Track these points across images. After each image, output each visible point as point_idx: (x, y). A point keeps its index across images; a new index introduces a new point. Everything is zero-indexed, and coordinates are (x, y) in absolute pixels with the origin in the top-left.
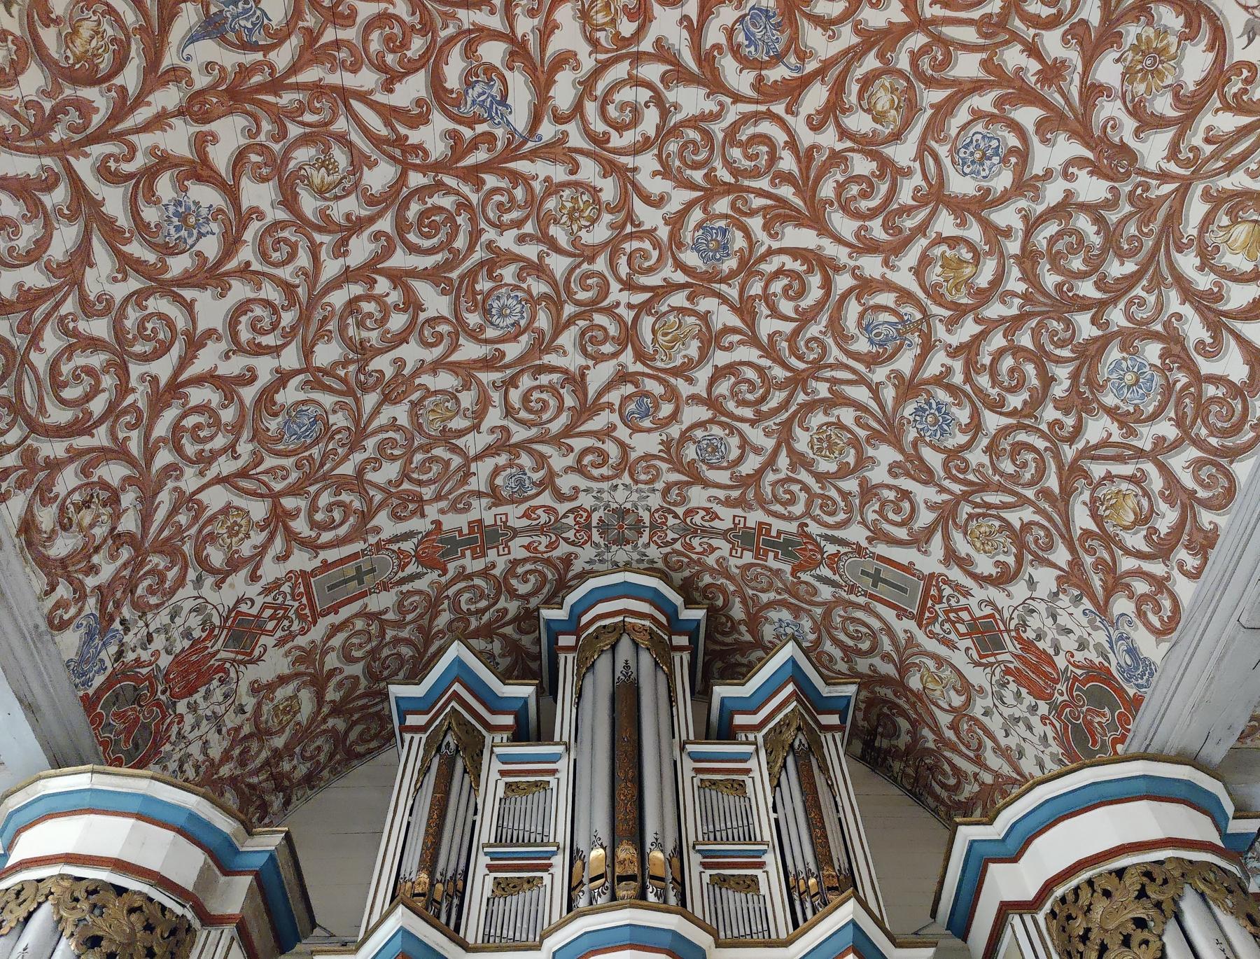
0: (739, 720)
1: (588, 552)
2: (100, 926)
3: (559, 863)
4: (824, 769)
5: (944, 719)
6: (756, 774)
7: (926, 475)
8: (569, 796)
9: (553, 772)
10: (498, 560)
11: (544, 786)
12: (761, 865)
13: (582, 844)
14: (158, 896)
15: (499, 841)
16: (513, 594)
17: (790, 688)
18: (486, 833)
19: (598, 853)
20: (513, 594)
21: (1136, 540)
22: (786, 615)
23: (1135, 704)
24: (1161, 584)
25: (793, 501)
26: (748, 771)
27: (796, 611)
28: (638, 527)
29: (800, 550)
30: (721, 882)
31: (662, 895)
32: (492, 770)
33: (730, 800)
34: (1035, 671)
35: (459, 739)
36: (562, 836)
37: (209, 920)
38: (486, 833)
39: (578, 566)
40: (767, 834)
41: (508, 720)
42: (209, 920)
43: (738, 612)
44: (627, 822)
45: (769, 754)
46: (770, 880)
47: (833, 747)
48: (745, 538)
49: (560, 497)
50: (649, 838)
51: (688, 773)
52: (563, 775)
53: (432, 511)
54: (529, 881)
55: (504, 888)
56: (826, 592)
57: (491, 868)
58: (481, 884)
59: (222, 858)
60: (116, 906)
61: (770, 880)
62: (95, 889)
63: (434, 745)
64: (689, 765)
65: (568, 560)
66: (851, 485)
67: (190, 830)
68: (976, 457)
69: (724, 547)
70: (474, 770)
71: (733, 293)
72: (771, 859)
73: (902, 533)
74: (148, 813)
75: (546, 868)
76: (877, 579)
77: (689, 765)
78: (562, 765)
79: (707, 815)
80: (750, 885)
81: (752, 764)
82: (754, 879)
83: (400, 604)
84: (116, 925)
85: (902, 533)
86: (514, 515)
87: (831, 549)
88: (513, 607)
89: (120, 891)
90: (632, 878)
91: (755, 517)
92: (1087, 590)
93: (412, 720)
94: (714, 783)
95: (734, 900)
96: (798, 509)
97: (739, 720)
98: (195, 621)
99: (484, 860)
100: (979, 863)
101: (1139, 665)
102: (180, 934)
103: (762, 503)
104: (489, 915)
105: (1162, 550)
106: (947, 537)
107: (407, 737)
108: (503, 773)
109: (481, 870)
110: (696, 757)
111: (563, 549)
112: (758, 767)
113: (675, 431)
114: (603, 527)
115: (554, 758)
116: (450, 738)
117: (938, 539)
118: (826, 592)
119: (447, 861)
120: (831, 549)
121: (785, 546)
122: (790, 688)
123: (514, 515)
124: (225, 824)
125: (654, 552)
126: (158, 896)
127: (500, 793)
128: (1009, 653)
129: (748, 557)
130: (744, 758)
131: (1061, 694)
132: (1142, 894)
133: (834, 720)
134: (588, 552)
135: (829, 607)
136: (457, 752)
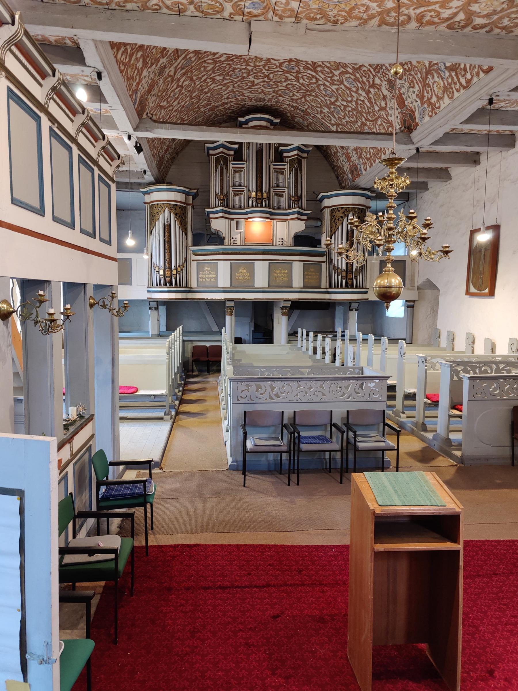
0: (285, 154)
1: (251, 103)
2: (177, 212)
3: (246, 190)
4: (301, 170)
5: (333, 151)
6: (286, 169)
7: (335, 117)
8: (248, 177)
9: (243, 168)
10: (227, 106)
11: (241, 171)
12: (284, 192)
13: (251, 189)
14: (182, 205)
15: (233, 186)
16: (230, 109)
17: (296, 152)
18: (231, 183)
19: (254, 194)
20: (230, 109)
21: (365, 154)
22: (301, 119)
23: (359, 175)
24: (366, 163)
25: (305, 105)
26: (284, 169)
27: (303, 120)
28: (265, 100)
29: (305, 112)
30: (276, 195)
31: (266, 202)
32: (230, 166)
33: (280, 176)
34: (349, 158)
35: (224, 162)
36: (246, 184)
37: (188, 204)
38: (231, 183)
39: (247, 105)
40: (287, 185)
41: (232, 153)
42: (188, 204)
43: (289, 115)
44: (259, 188)
45: (290, 165)
46: (286, 195)
47: (304, 163)
48: (293, 107)
49: (245, 96)
50: (264, 190)
51: (272, 169)
52: (246, 169)
53: (212, 104)
54: (240, 194)
55: (236, 195)
56: (311, 121)
57: (233, 191)
58: (231, 194)
59: (187, 194)
60: (177, 208)
61: (286, 195)
62: (174, 205)
63: (217, 161)
64: (272, 167)
65: (245, 104)
66: (319, 109)
67: (182, 192)
68: (344, 121)
69: (287, 107)
70: (227, 168)
71: (295, 75)
72: (286, 190)
73: (329, 121)
74: (176, 191)
75: (243, 191)
76: (322, 124)
77: (272, 167)
78: (245, 166)
79: (275, 179)
80: (282, 196)
81: (286, 167)
82: (283, 194)
83: (203, 118)
84: (178, 211)
85: (329, 121)
86: (232, 100)
87: (312, 115)
88: (230, 111)
89: (177, 205)
90: (260, 199)
91: (294, 105)
92: (357, 154)
93: (211, 152)
94: (277, 172)
95: (278, 198)
96: (306, 107)
97: (285, 154)
98: (168, 144)
99: (231, 189)
100: (323, 198)
101: (361, 170)
102: (185, 208)
103: (297, 103)
104: (233, 200)
105: (368, 159)
106: (337, 127)
107: (210, 156)
108: (233, 167)
109: (231, 191)
110: (274, 165)
111: (244, 103)
112: (287, 167)
113: (277, 89)
114: (255, 100)
115: (243, 164)
116: (222, 163)
117: (335, 127)
118: (311, 121)
119: (225, 192)
120: (312, 115)
121: (302, 111)
122: (296, 152)
123: (232, 100)
124: (187, 190)
125: (268, 103)
126: (182, 205)
127: (233, 173)
128: (345, 151)
129: (292, 109)
130: (284, 165)
131: (351, 164)
132: (344, 213)
133: (305, 155)
134: (251, 103)
135: (311, 123)
136: (222, 162)
